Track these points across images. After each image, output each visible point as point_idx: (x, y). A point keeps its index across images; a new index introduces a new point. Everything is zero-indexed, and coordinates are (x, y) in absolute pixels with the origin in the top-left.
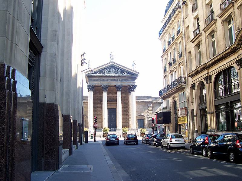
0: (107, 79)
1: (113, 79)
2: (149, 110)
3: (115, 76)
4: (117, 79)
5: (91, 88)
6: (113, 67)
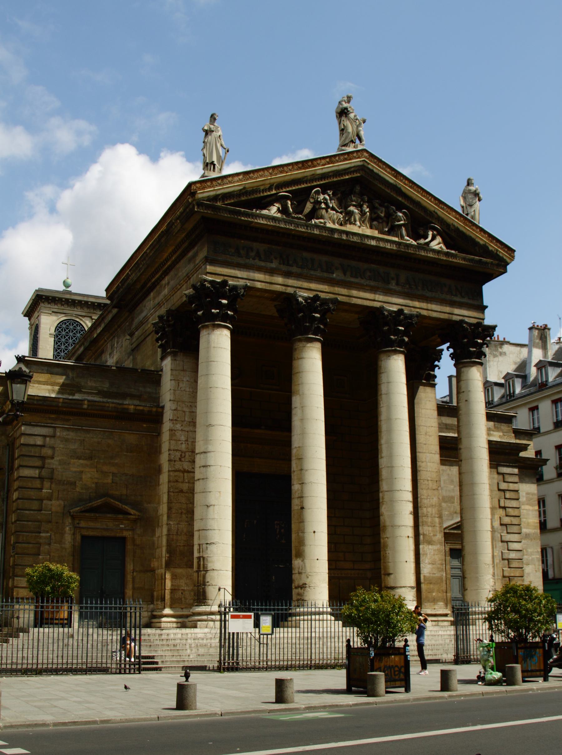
0: (324, 258)
2: (508, 495)
3: (382, 245)
5: (225, 302)
6: (365, 183)
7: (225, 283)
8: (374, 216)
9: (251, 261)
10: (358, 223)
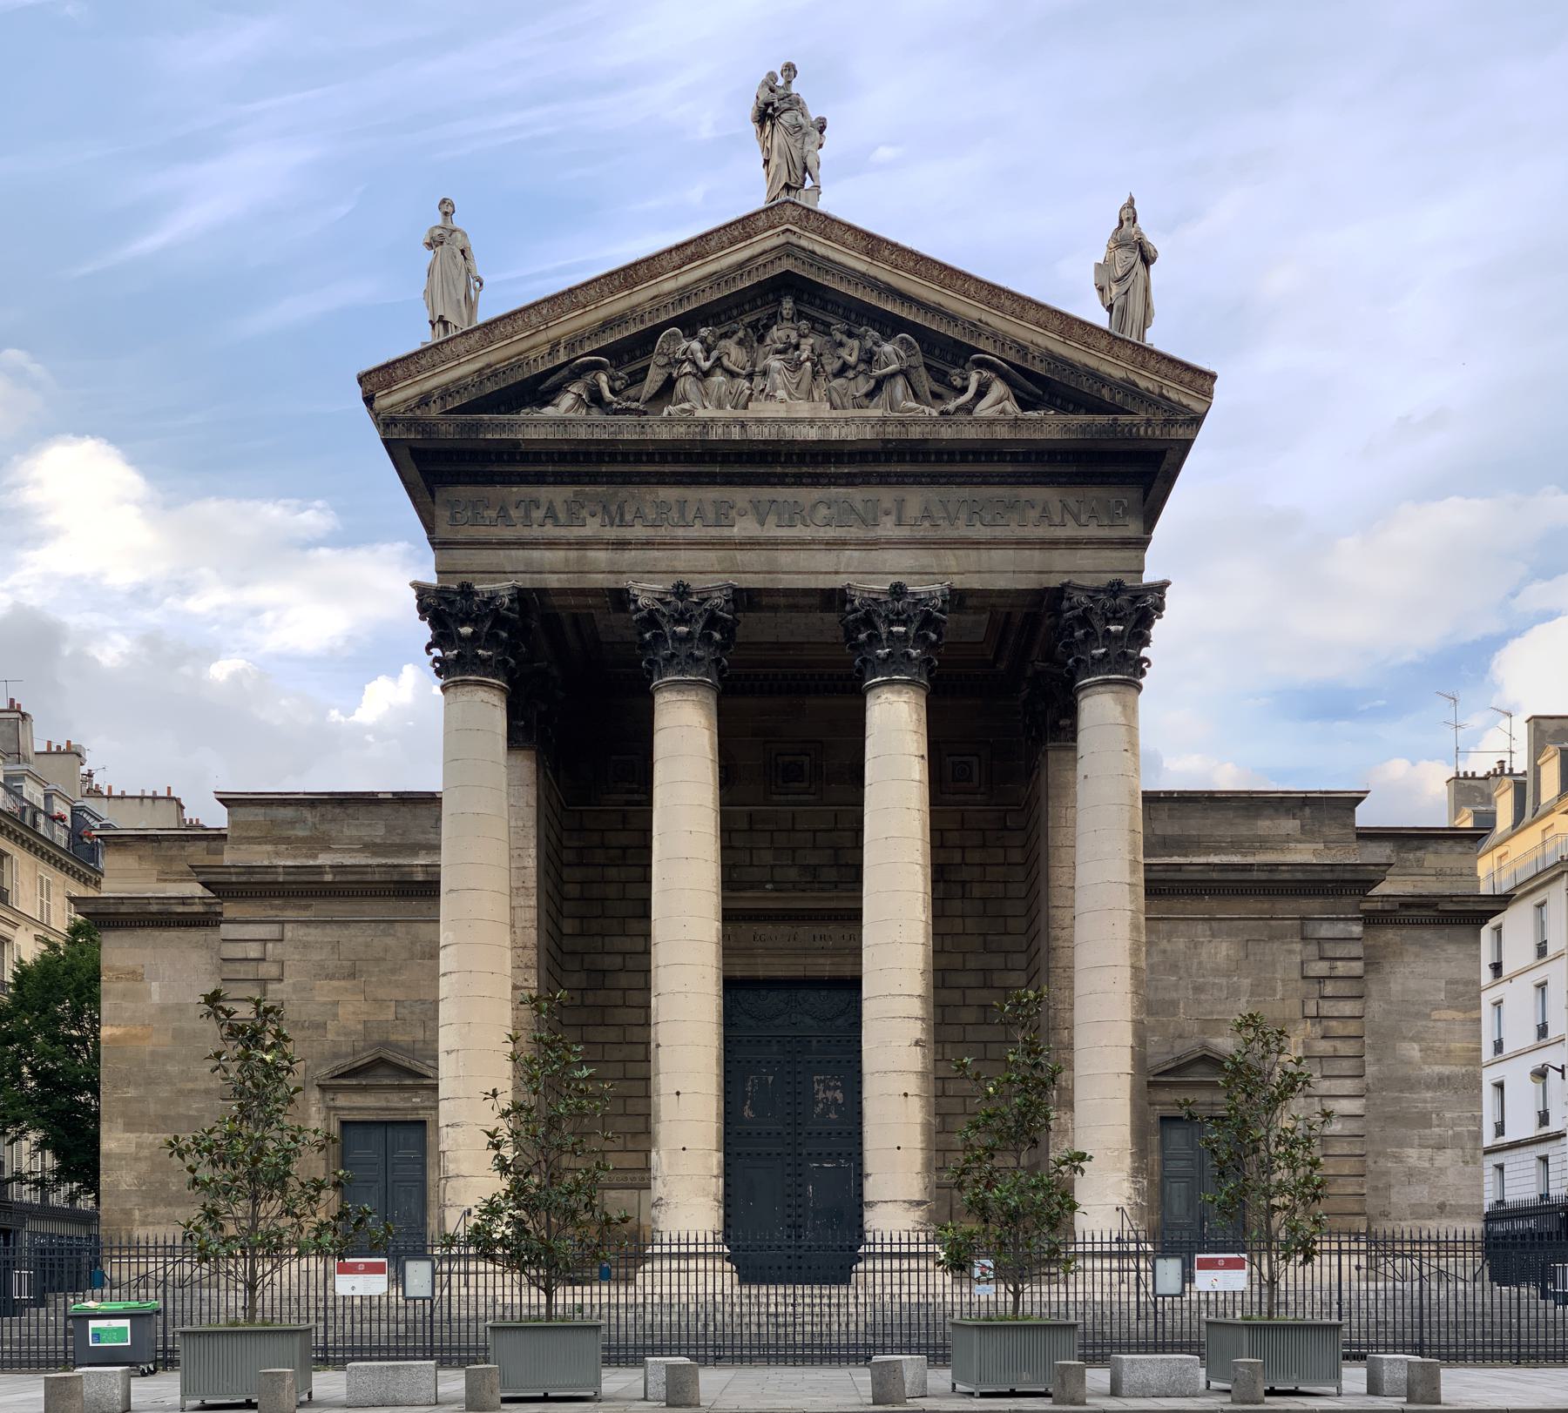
0: (711, 494)
1: (817, 493)
4: (856, 495)
7: (466, 591)
8: (837, 364)
9: (535, 532)
10: (781, 394)
